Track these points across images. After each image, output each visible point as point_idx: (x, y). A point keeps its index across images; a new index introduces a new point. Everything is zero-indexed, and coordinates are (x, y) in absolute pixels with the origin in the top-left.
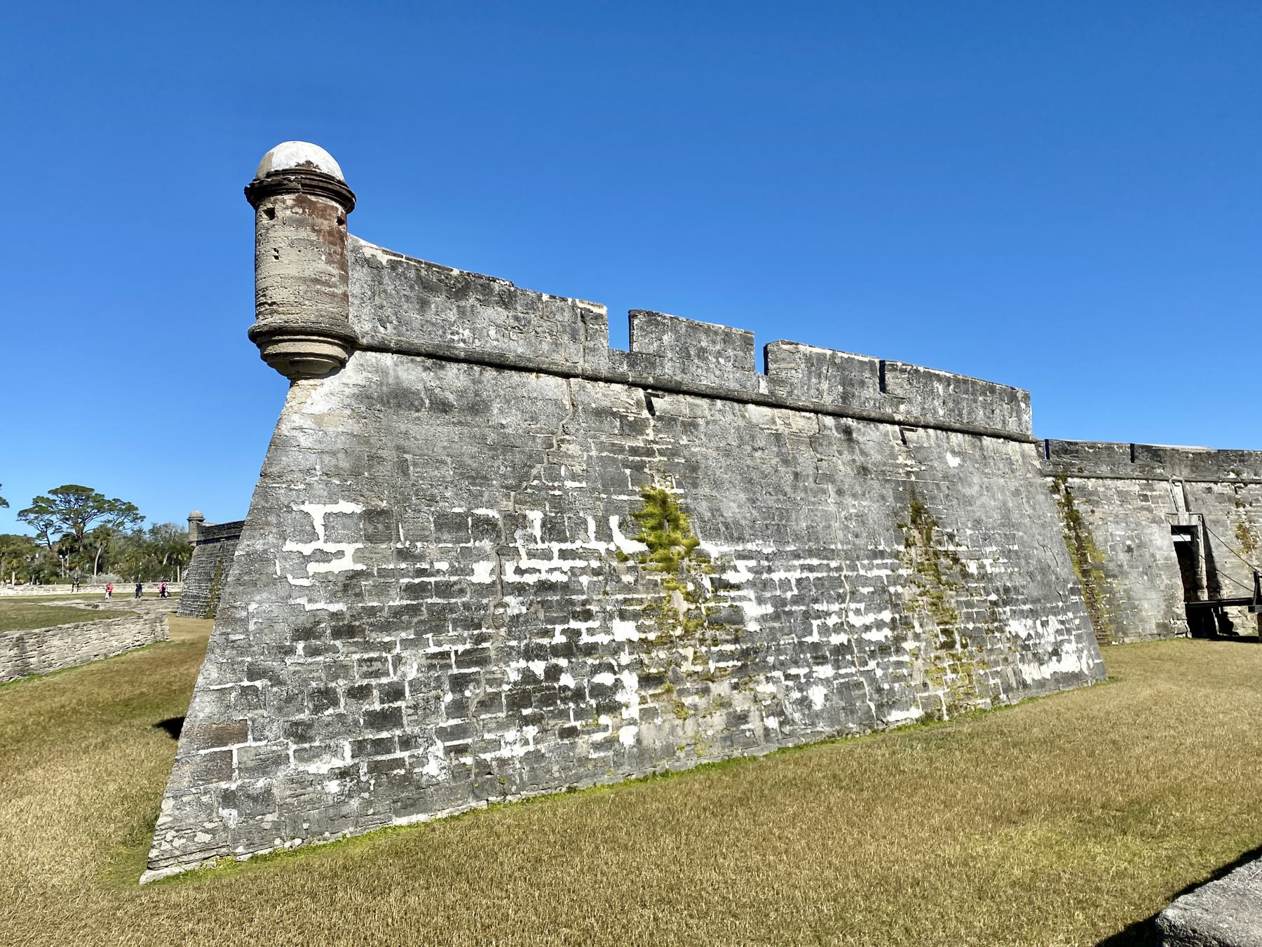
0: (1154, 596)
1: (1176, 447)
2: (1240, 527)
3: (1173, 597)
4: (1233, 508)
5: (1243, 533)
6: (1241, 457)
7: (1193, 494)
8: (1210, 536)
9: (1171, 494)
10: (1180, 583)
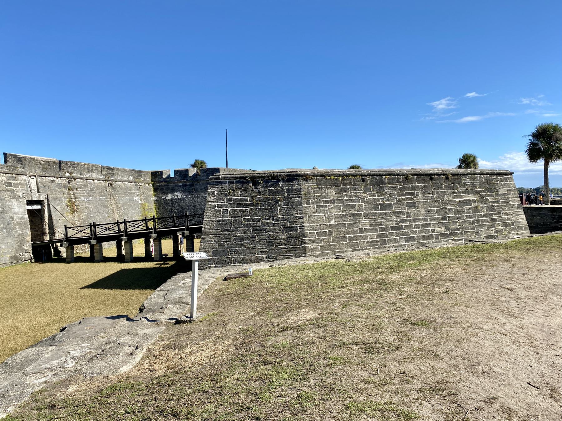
0: (10, 241)
1: (33, 157)
2: (70, 201)
3: (23, 240)
4: (67, 191)
5: (71, 204)
6: (73, 165)
7: (43, 183)
8: (51, 206)
9: (30, 184)
10: (29, 232)
